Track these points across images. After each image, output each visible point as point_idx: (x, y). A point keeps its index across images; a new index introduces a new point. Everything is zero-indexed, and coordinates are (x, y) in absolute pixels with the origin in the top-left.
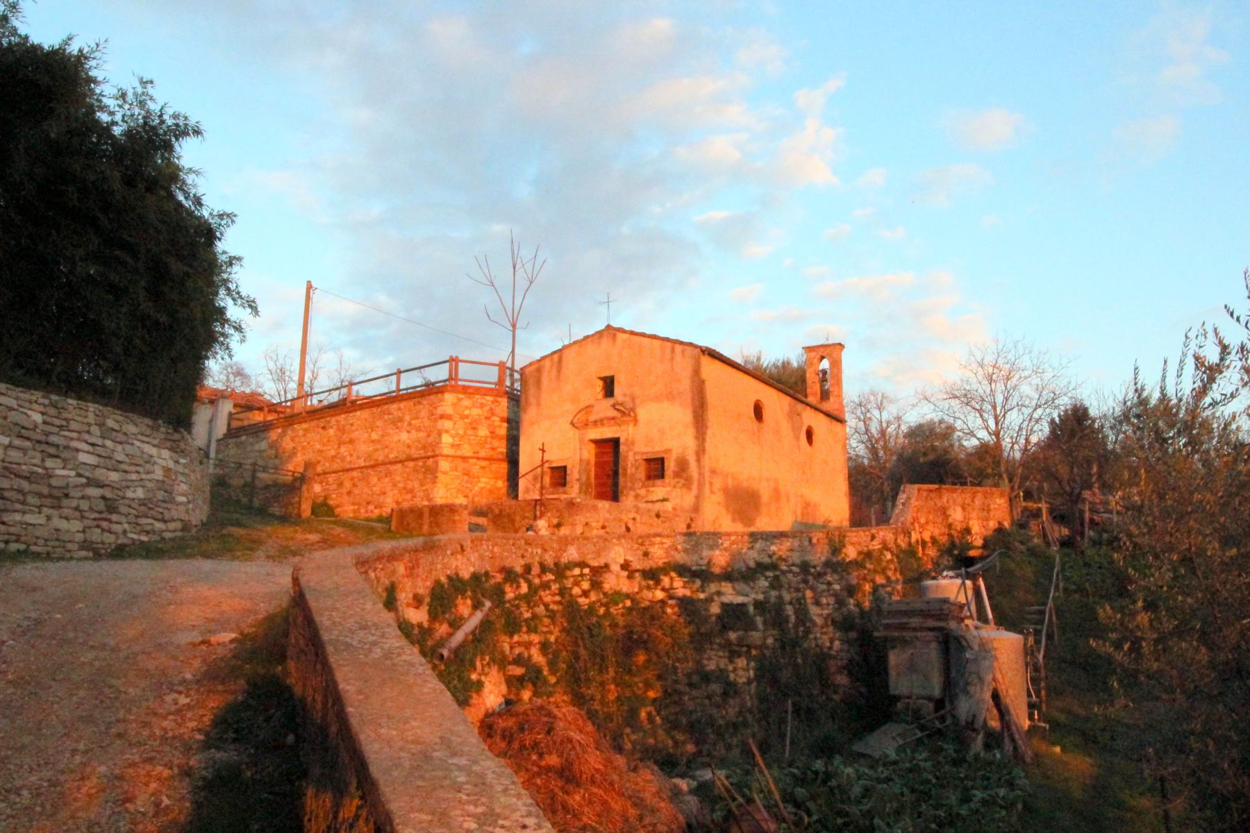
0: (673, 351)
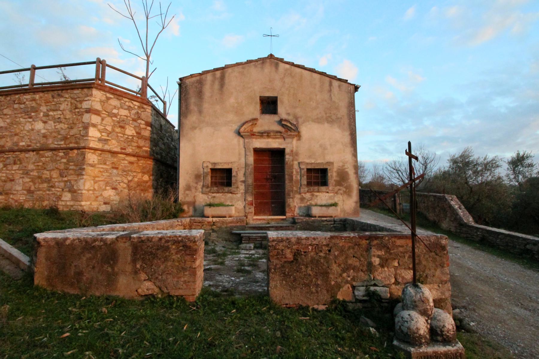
0: (331, 84)
